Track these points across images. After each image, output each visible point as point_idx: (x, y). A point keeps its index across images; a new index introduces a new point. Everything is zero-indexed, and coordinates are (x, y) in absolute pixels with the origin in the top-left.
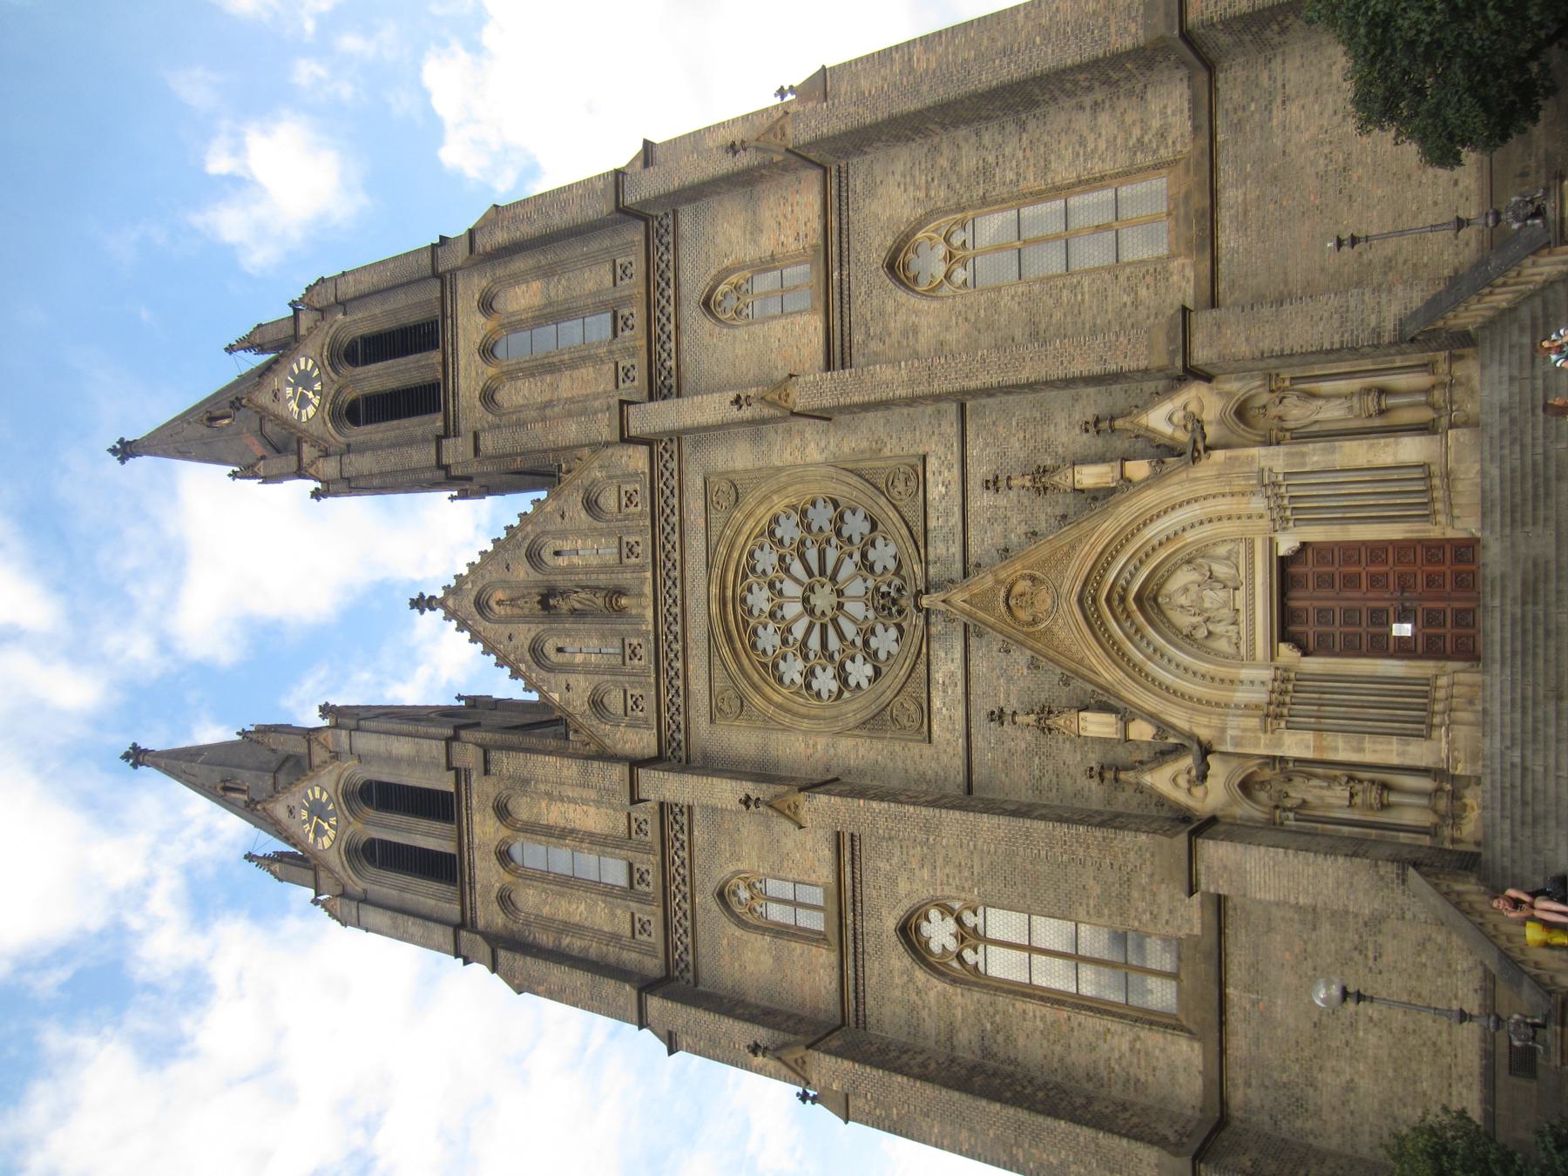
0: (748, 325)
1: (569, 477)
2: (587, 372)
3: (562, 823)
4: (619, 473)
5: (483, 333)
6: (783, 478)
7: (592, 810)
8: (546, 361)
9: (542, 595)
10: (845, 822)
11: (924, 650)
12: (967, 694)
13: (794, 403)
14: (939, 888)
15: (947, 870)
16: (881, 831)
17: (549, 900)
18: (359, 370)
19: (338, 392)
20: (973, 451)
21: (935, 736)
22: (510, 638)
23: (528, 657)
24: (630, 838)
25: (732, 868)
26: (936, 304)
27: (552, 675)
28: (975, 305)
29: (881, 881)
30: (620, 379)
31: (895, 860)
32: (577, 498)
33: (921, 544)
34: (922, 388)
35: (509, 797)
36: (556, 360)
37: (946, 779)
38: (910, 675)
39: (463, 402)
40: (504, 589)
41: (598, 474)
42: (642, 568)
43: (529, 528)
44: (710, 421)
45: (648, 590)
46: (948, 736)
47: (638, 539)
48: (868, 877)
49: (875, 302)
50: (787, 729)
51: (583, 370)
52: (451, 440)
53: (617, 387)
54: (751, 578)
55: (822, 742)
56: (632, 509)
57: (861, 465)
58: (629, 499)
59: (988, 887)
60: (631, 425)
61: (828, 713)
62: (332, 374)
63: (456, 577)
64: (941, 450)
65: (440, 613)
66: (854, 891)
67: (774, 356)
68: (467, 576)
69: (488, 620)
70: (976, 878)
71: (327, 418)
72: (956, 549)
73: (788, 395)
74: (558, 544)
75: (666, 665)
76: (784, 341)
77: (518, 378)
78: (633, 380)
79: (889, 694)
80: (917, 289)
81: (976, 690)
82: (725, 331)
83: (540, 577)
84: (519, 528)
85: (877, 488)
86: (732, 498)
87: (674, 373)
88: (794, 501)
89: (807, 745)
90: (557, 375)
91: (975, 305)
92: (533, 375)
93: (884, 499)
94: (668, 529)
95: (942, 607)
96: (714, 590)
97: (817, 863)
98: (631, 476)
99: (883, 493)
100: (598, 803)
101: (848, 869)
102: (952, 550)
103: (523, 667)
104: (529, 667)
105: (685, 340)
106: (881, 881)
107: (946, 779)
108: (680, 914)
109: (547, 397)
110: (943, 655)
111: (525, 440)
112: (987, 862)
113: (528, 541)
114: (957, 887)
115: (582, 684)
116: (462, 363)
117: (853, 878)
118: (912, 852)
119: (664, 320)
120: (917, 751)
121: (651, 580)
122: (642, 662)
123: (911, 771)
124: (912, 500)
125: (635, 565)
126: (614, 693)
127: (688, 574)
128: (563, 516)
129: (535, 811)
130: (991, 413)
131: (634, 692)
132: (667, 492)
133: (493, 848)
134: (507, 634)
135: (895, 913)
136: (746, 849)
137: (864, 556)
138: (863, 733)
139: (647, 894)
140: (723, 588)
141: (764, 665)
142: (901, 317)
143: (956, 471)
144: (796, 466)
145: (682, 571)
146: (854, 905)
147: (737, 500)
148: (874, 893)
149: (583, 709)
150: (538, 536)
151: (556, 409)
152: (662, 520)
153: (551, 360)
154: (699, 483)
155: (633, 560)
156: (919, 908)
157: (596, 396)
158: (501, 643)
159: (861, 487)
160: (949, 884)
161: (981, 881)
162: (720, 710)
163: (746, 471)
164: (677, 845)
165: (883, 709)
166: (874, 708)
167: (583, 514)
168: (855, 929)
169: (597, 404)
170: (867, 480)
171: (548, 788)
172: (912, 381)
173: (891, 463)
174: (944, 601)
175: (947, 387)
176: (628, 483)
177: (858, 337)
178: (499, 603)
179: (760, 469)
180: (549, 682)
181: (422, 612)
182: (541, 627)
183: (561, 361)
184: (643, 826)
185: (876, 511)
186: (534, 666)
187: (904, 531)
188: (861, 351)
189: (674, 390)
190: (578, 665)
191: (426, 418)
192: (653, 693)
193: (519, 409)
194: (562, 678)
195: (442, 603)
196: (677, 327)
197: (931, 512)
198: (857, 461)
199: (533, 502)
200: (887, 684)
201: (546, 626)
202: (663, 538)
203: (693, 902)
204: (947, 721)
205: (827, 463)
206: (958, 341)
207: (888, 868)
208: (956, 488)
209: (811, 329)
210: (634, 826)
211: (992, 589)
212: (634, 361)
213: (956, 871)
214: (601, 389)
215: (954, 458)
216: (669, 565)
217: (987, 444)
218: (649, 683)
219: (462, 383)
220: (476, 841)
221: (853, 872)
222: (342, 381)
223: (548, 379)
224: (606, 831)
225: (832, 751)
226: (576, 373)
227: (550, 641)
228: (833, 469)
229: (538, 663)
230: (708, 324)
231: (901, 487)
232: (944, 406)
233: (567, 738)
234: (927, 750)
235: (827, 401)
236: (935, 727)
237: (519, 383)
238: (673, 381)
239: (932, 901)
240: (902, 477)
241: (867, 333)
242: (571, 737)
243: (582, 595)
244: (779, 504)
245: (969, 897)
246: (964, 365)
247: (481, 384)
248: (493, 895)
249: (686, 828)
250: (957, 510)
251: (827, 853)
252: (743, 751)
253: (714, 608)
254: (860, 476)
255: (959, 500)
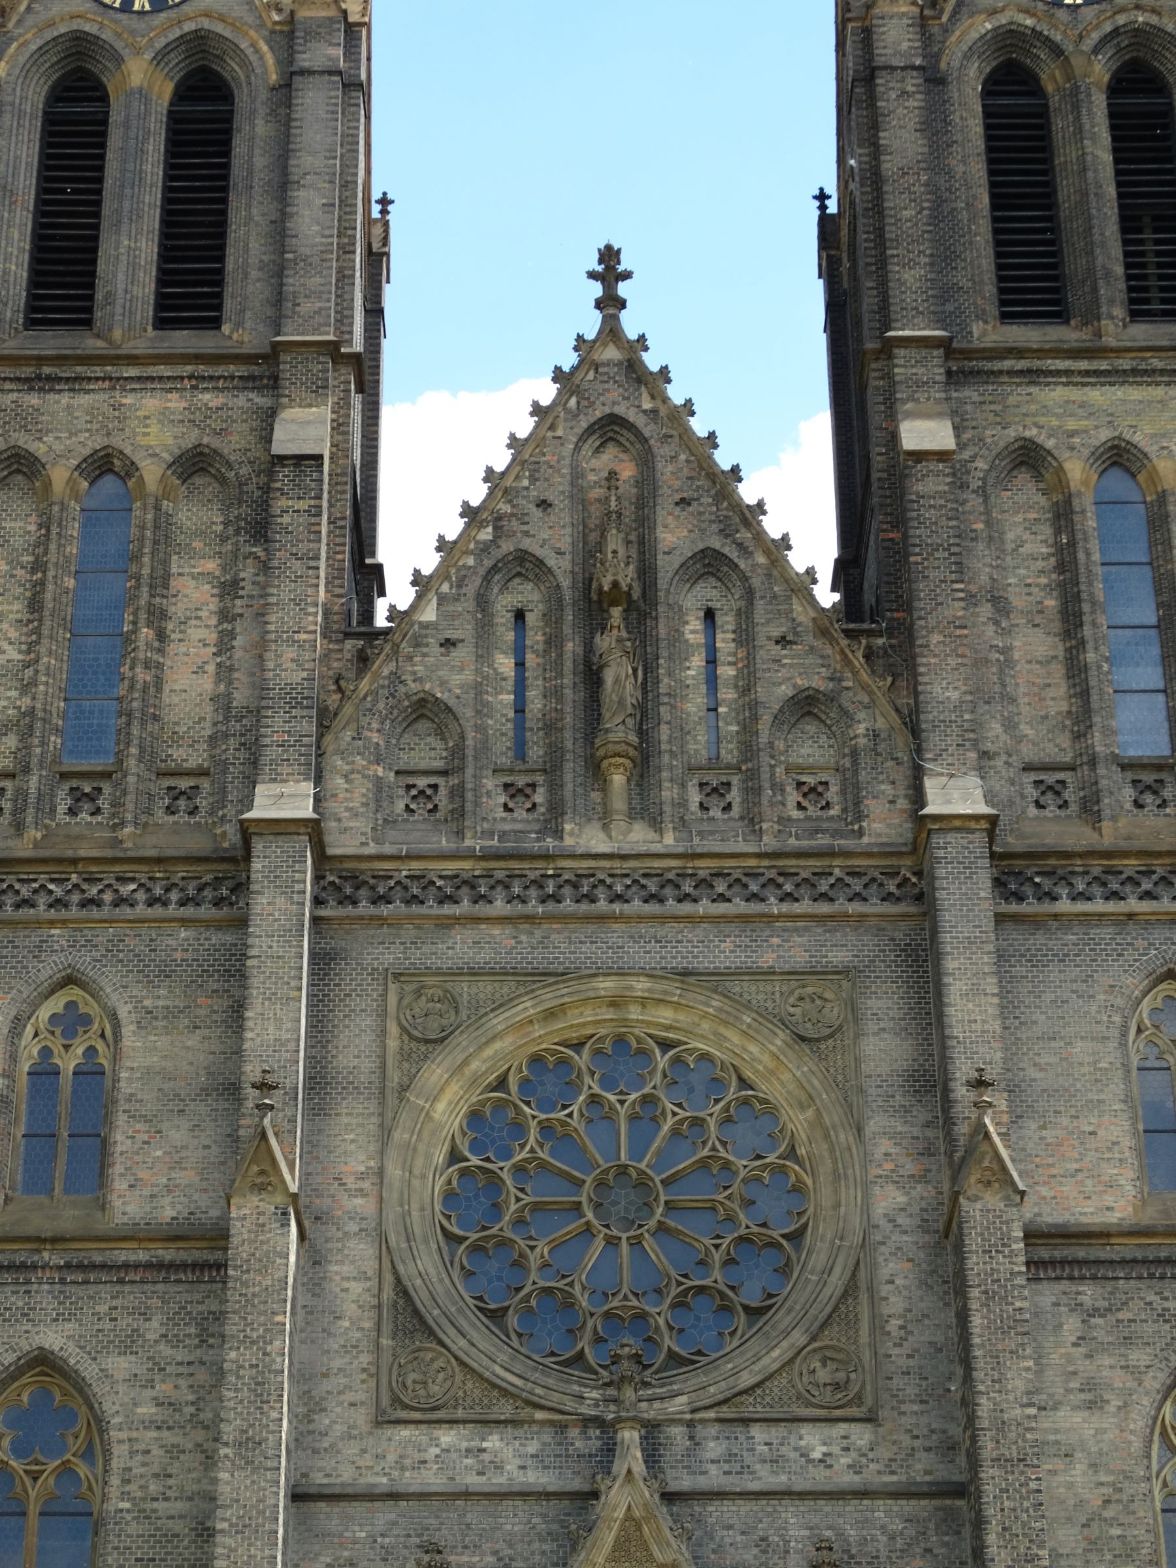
0: (1126, 1068)
1: (858, 660)
2: (1058, 699)
3: (178, 609)
4: (863, 776)
5: (1151, 449)
6: (845, 1137)
7: (207, 684)
8: (1086, 607)
9: (629, 594)
10: (245, 1284)
11: (539, 1415)
12: (467, 1495)
13: (976, 1198)
14: (123, 1435)
15: (156, 1451)
16: (233, 1355)
17: (20, 572)
18: (1098, 105)
19: (1057, 51)
20: (881, 1511)
21: (389, 1431)
22: (544, 504)
23: (507, 546)
24: (161, 774)
25: (123, 1011)
26: (1137, 1445)
27: (470, 605)
28: (1131, 1519)
29: (126, 1322)
30: (1042, 776)
31: (165, 1350)
32: (818, 682)
33: (726, 1412)
34: (990, 1445)
35: (223, 481)
36: (1087, 631)
37: (315, 1451)
38: (494, 1386)
39: (1018, 395)
40: (639, 484)
41: (861, 729)
42: (682, 824)
43: (761, 559)
44: (950, 1011)
45: (639, 837)
46: (391, 1458)
47: (736, 811)
48: (131, 1297)
49: (1149, 1328)
50: (385, 1133)
51: (1062, 690)
52: (939, 373)
53: (1028, 768)
54: (662, 1061)
55: (364, 1205)
56: (793, 796)
57: (864, 1297)
58: (813, 790)
59: (133, 1529)
60: (951, 837)
61: (415, 1214)
62: (1096, 36)
63: (664, 372)
64: (884, 1453)
65: (591, 324)
66: (103, 1267)
67: (1065, 1121)
68: (666, 400)
69: (577, 448)
70: (149, 1506)
71: (1003, 19)
72: (714, 1478)
73: (989, 1184)
74: (726, 621)
75: (500, 875)
76: (1092, 1143)
77: (1058, 532)
78: (1039, 805)
79: (459, 1344)
80: (1168, 1403)
81: (474, 1513)
82: (1117, 1019)
83: (664, 578)
84: (760, 534)
85: (822, 1327)
86: (809, 1030)
87: (1047, 907)
88: (802, 1151)
89: (361, 1177)
90: (1057, 626)
91: (1123, 1519)
92: (1061, 568)
93: (803, 1340)
94: (754, 887)
95: (619, 1467)
96: (641, 986)
97: (147, 1192)
98: (857, 804)
99: (813, 1339)
100: (222, 702)
101: (142, 1256)
102: (713, 1470)
103: (486, 534)
104: (484, 549)
105: (1105, 932)
106: (126, 1322)
107: (315, 1451)
108: (25, 892)
109: (1018, 601)
110: (532, 1448)
111: (932, 574)
112: (178, 1526)
113: (733, 554)
114: (130, 1469)
115: (456, 679)
116: (1096, 395)
117: (126, 1266)
118: (183, 1383)
119: (1146, 885)
120: (361, 1396)
121: (657, 848)
122: (500, 813)
123: (327, 1385)
124: (799, 1396)
125: (683, 803)
126: (438, 744)
127: (668, 931)
128: (782, 641)
129: (197, 544)
130: (946, 1545)
131: (443, 791)
132: (823, 885)
133: (117, 441)
134: (550, 496)
135: (71, 1347)
136: (163, 1042)
137: (701, 1289)
138: (388, 1294)
139: (53, 810)
140: (643, 1002)
141: (501, 1084)
142: (1120, 1379)
143: (848, 1480)
144: (864, 1168)
145: (676, 918)
146: (80, 1267)
147: (803, 1039)
148: (103, 1308)
149: (408, 677)
150: (745, 579)
151: (990, 630)
152: (772, 874)
153: (1086, 618)
154: (839, 957)
155: (695, 797)
156: (81, 1391)
157: (1010, 725)
158: (533, 479)
159: (828, 1291)
160: (132, 1453)
161: (145, 1516)
162: (418, 993)
163: (858, 1060)
164: (158, 891)
165: (431, 1333)
166: (432, 1314)
167: (785, 691)
168: (34, 1267)
169: (995, 728)
170: (836, 1308)
171: (248, 589)
172: (1002, 1427)
173: (867, 1356)
174: (629, 1472)
175: (989, 1491)
176: (843, 792)
177: (1089, 1293)
178: (612, 475)
179: (861, 1091)
180: (457, 599)
181: (592, 275)
182: (565, 583)
183: (1082, 643)
184: (182, 803)
185: (782, 1319)
186: (488, 563)
187: (746, 1380)
188: (1064, 1300)
189: (1014, 908)
190: (490, 666)
191: (990, 289)
192: (445, 843)
193: (995, 537)
194: (464, 630)
195: (611, 330)
196: (1131, 916)
197: (775, 1433)
198: (871, 1289)
199: (810, 573)
200: (474, 1335)
201: (568, 594)
202: (737, 874)
203: (52, 923)
204: (418, 1456)
205: (870, 1226)
206: (1070, 1486)
207: (151, 1336)
208: (818, 1478)
209: (1109, 1200)
210: (184, 784)
211: (651, 1558)
212: (1074, 807)
213: (156, 1470)
214: (1025, 729)
215: (873, 1475)
216: (687, 887)
217: (892, 1538)
218: (460, 834)
219: (1056, 394)
220: (128, 400)
221: (137, 1266)
222: (1077, 62)
223: (1051, 603)
224: (169, 717)
225: (353, 1227)
226: (1058, 671)
227: (536, 596)
228: (857, 1239)
229: (494, 569)
230: (1134, 983)
231: (823, 1375)
232: (962, 1460)
233: (348, 635)
234: (362, 1418)
235: (975, 1264)
236: (405, 1432)
237: (1047, 531)
238: (1030, 907)
239: (99, 1421)
240: (841, 1376)
241: (1095, 1312)
242: (349, 644)
243: (629, 686)
244: (797, 1121)
245: (114, 1491)
246: (1024, 1525)
247: (1050, 444)
248: (24, 440)
249: (189, 911)
250: (781, 1480)
251: (168, 1211)
252: (342, 1040)
253: (606, 985)
254: (845, 1295)
255: (799, 1485)
